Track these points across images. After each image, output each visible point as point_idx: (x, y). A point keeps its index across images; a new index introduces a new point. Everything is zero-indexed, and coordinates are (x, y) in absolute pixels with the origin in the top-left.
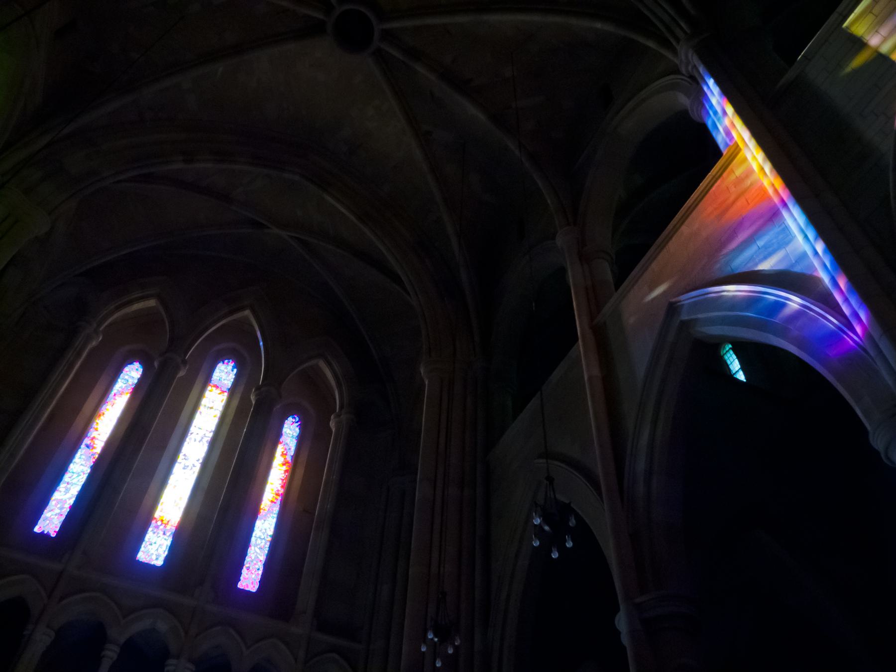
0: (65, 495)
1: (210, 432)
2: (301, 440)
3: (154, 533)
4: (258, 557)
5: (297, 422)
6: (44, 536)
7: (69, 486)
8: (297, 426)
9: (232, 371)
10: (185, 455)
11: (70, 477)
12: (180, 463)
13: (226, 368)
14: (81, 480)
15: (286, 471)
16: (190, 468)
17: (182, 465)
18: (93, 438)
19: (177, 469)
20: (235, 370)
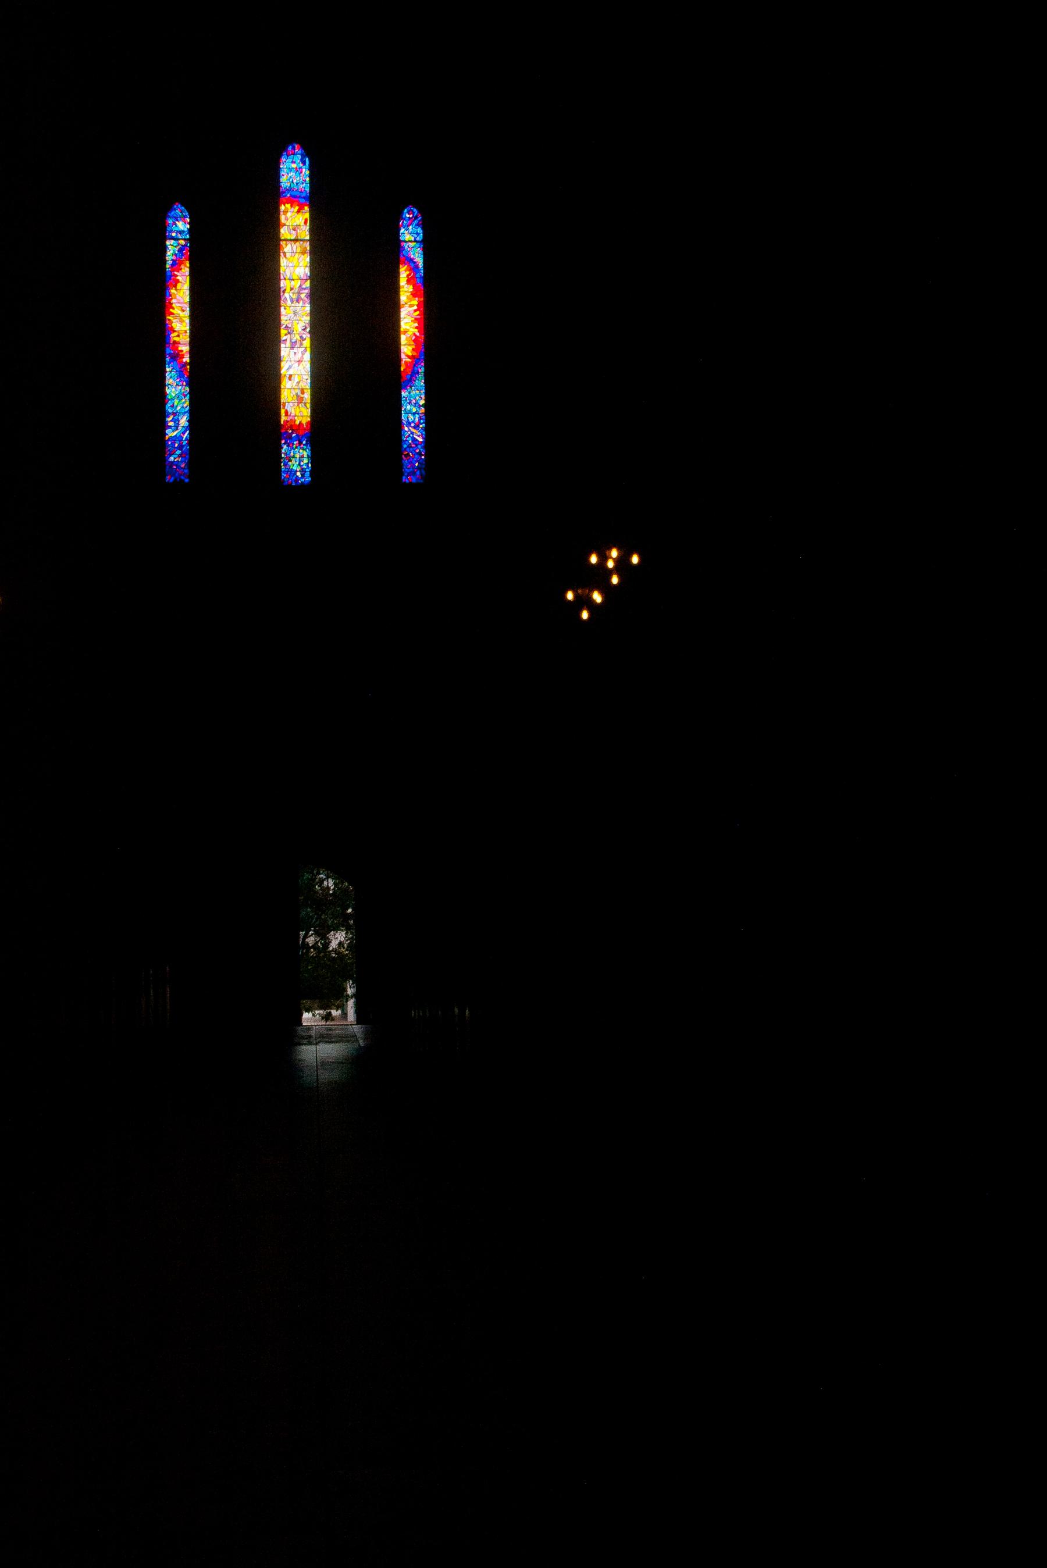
0: (177, 429)
1: (307, 280)
2: (428, 245)
3: (288, 446)
4: (417, 440)
5: (416, 218)
6: (178, 483)
7: (176, 417)
8: (418, 225)
9: (304, 163)
10: (287, 327)
11: (172, 406)
12: (286, 340)
13: (294, 162)
14: (185, 405)
15: (419, 302)
16: (298, 345)
17: (288, 344)
18: (175, 342)
19: (285, 351)
20: (307, 160)
